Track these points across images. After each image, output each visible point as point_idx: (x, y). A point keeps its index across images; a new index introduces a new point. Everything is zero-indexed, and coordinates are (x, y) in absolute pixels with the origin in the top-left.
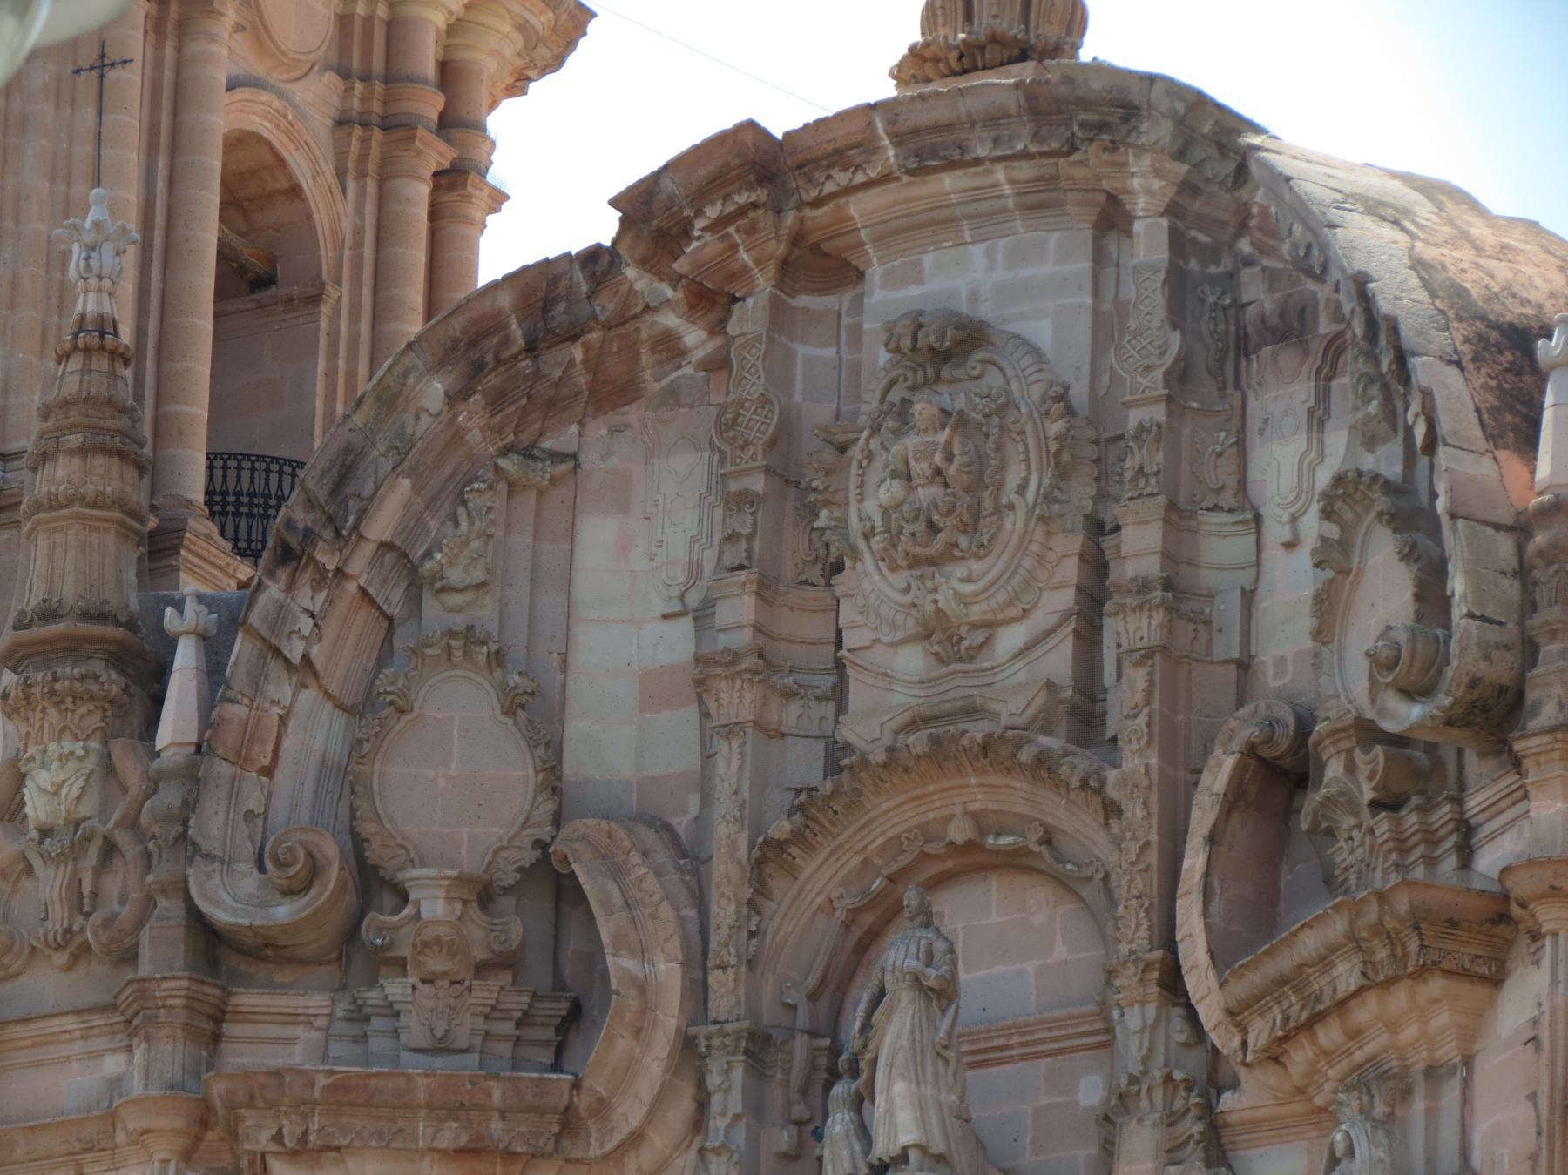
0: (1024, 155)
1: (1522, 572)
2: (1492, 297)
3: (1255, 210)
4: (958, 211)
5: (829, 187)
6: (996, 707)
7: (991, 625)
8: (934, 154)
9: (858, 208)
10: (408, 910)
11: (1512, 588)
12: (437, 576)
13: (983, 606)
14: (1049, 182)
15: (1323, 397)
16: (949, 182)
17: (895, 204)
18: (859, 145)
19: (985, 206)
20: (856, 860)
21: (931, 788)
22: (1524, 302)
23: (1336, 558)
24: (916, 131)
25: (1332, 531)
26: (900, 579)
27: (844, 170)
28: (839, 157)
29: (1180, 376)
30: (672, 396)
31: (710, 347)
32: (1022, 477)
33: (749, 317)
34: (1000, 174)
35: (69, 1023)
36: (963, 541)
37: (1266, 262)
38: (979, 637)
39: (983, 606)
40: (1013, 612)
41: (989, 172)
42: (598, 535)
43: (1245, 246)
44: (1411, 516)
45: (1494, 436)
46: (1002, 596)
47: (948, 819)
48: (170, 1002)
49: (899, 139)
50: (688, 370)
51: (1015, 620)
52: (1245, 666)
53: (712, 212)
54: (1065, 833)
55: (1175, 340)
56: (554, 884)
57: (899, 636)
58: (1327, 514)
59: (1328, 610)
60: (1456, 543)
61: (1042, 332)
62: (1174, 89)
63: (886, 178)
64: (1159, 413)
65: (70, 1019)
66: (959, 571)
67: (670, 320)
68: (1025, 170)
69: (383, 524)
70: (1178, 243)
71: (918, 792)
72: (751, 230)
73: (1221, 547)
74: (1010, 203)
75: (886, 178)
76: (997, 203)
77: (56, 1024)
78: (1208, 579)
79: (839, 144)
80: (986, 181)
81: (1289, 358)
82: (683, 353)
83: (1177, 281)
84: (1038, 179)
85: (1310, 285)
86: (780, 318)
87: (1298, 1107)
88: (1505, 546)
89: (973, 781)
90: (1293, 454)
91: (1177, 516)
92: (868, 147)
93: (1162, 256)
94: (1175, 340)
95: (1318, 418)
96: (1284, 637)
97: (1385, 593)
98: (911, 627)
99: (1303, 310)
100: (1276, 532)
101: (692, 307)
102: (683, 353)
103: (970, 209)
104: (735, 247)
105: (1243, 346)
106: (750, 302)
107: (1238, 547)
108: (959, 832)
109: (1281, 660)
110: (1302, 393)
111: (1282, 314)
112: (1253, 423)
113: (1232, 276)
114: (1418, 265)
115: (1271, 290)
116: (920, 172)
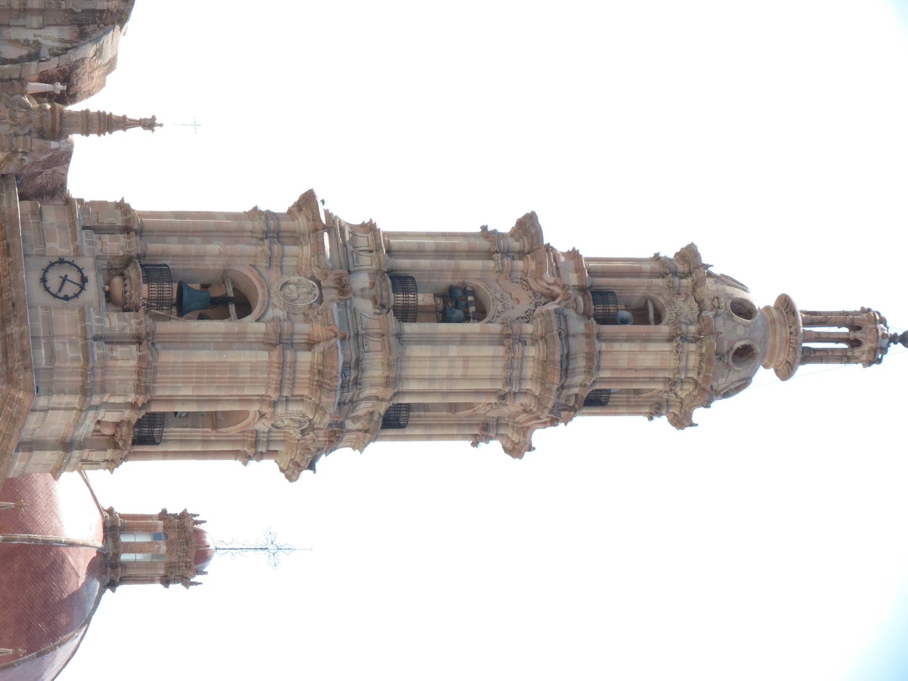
1: (10, 79)
2: (77, 75)
11: (7, 77)
15: (67, 42)
22: (77, 82)
23: (26, 43)
25: (31, 43)
29: (72, 12)
43: (102, 25)
44: (31, 57)
45: (41, 74)
52: (9, 26)
55: (79, 11)
58: (35, 41)
59: (16, 42)
60: (17, 66)
62: (130, 10)
64: (63, 7)
70: (102, 11)
73: (36, 21)
78: (28, 18)
81: (75, 35)
83: (94, 11)
88: (16, 76)
90: (51, 36)
93: (98, 8)
94: (79, 11)
95: (61, 40)
96: (14, 33)
97: (13, 52)
100: (38, 32)
105: (80, 25)
107: (35, 25)
110: (67, 37)
112: (63, 27)
113: (96, 23)
114: (83, 59)
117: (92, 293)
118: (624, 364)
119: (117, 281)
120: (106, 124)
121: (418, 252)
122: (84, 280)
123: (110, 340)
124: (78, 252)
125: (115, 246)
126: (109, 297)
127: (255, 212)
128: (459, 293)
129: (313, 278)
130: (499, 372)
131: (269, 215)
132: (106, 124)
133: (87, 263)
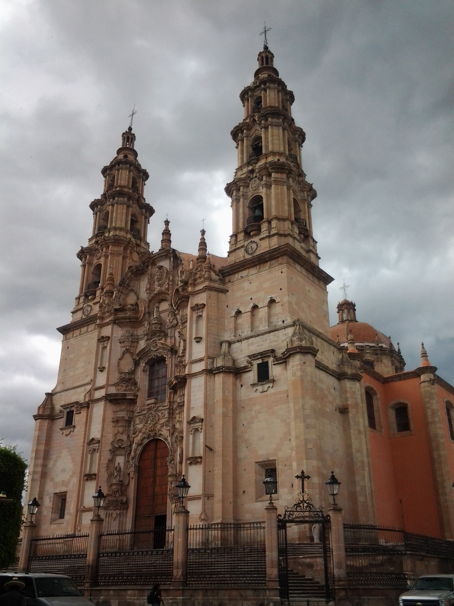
32: (165, 275)
33: (149, 268)
42: (142, 283)
56: (137, 304)
61: (166, 266)
69: (127, 283)
86: (152, 268)
91: (173, 276)
117: (256, 239)
118: (274, 101)
119: (251, 234)
120: (203, 245)
121: (242, 159)
122: (251, 241)
123: (270, 229)
124: (242, 247)
125: (241, 236)
126: (256, 235)
127: (232, 206)
128: (255, 146)
129: (250, 181)
130: (277, 128)
131: (232, 203)
132: (203, 245)
133: (246, 243)
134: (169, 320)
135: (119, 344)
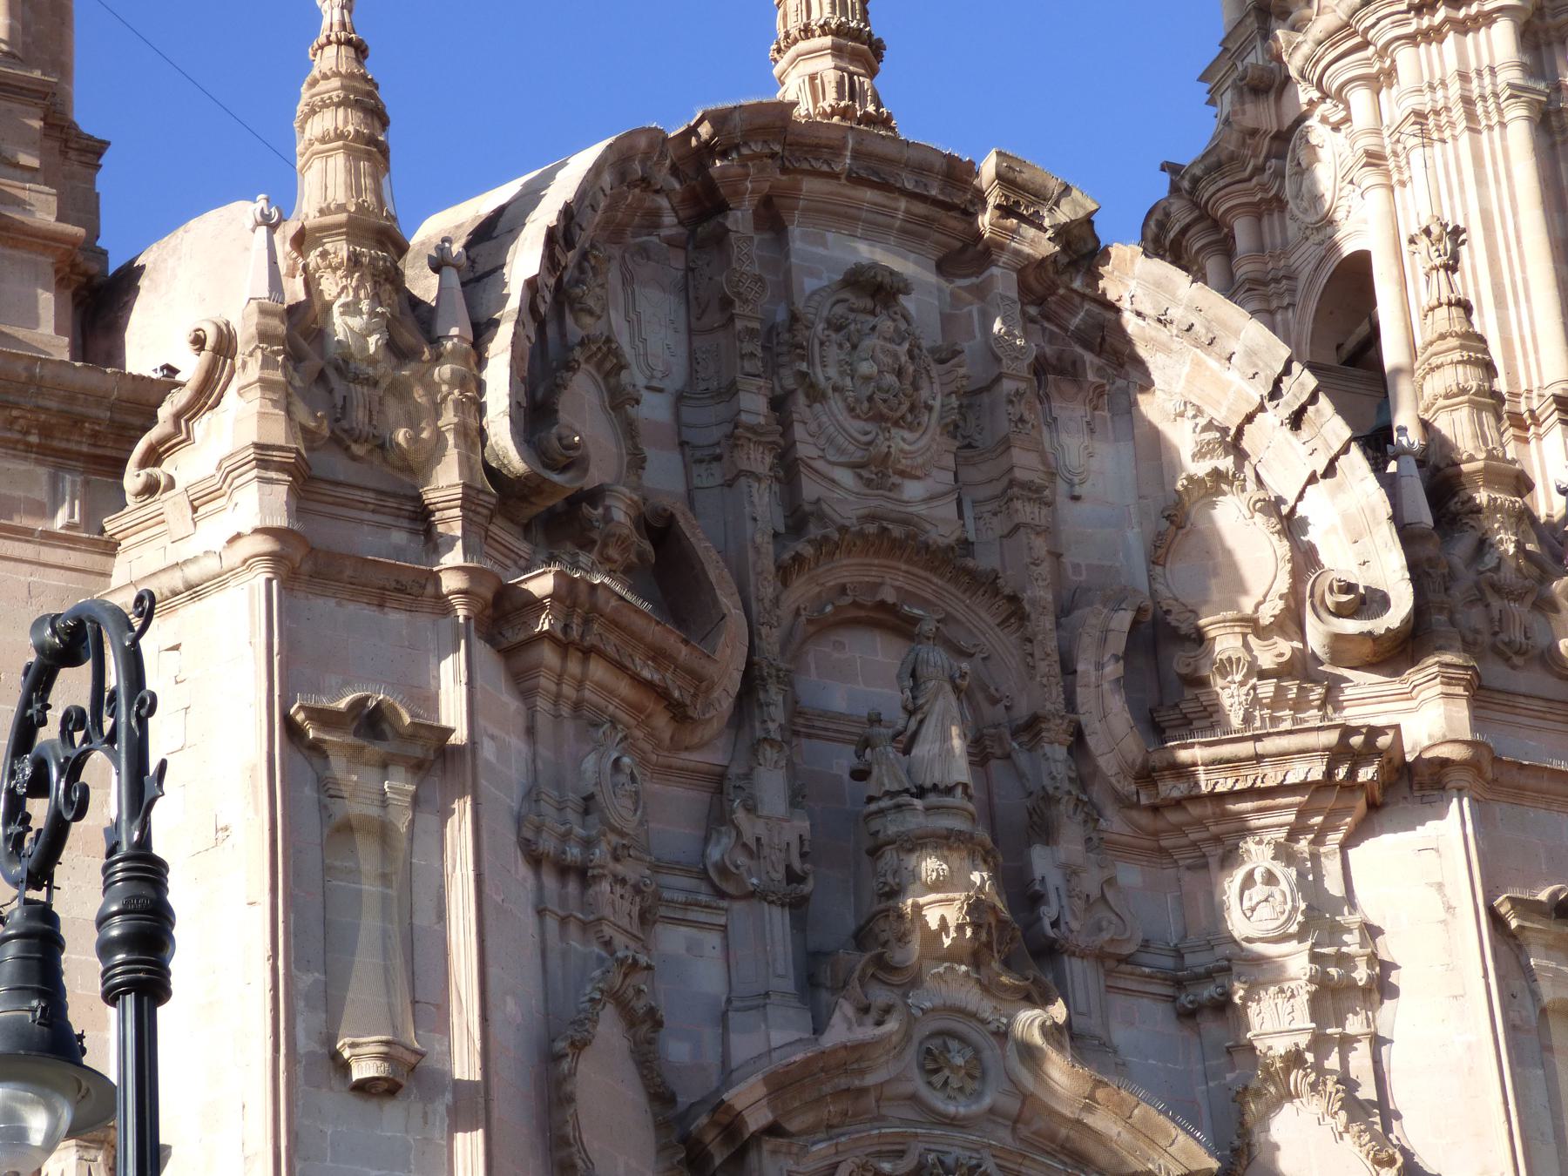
0: (923, 198)
3: (1061, 291)
4: (864, 215)
5: (806, 166)
6: (928, 527)
7: (903, 474)
8: (876, 173)
9: (809, 185)
10: (601, 510)
12: (580, 300)
13: (909, 462)
14: (928, 221)
16: (869, 195)
17: (831, 193)
18: (831, 148)
19: (881, 219)
20: (818, 589)
21: (876, 562)
24: (870, 155)
26: (868, 427)
27: (817, 159)
28: (815, 149)
30: (644, 252)
31: (673, 231)
34: (903, 204)
35: (369, 497)
36: (909, 418)
37: (1046, 324)
38: (896, 479)
39: (909, 462)
40: (918, 473)
41: (896, 199)
46: (920, 460)
47: (876, 587)
48: (480, 509)
49: (856, 155)
50: (655, 239)
51: (918, 478)
53: (757, 147)
54: (957, 621)
57: (842, 459)
63: (836, 176)
65: (371, 495)
66: (907, 434)
67: (664, 202)
68: (920, 208)
71: (867, 561)
72: (761, 170)
74: (898, 223)
75: (836, 176)
76: (889, 220)
77: (358, 495)
79: (824, 142)
80: (893, 204)
82: (658, 226)
84: (926, 217)
85: (1079, 350)
87: (1146, 843)
89: (904, 567)
92: (837, 150)
98: (858, 456)
99: (1074, 363)
101: (683, 201)
102: (658, 226)
103: (871, 216)
104: (748, 175)
106: (739, 214)
108: (889, 596)
109: (1076, 567)
111: (1059, 359)
115: (1050, 342)
116: (856, 180)
134: (1071, 872)
135: (523, 870)
